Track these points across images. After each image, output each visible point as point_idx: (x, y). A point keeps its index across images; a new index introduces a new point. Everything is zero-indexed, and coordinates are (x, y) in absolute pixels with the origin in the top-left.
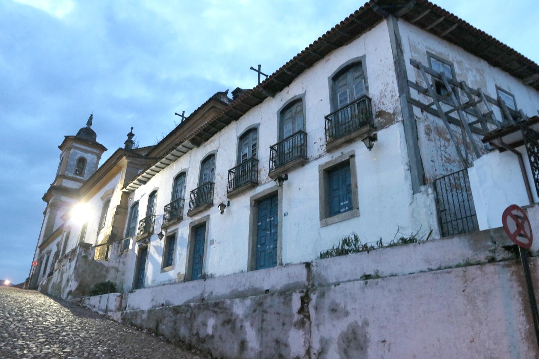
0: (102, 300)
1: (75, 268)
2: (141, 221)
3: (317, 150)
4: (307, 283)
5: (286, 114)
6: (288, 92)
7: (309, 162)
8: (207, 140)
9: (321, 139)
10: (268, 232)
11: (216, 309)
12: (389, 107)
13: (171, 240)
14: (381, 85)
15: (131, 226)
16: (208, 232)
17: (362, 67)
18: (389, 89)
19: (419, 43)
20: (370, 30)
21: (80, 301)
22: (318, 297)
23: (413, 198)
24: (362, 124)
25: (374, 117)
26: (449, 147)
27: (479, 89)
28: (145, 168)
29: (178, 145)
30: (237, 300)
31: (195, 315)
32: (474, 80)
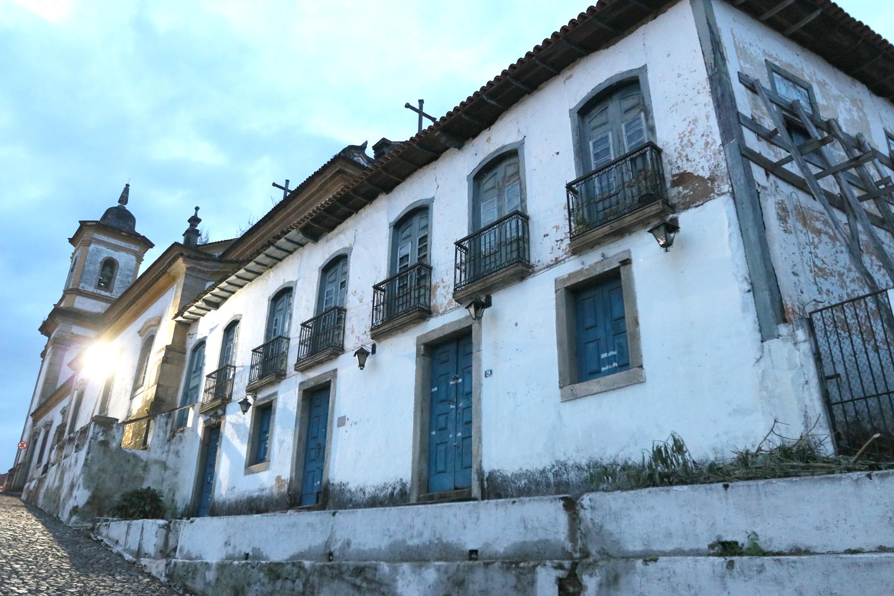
0: (131, 531)
1: (85, 465)
2: (209, 376)
3: (550, 250)
4: (569, 546)
5: (484, 181)
6: (488, 140)
7: (533, 272)
8: (332, 228)
9: (557, 227)
10: (452, 407)
11: (358, 581)
12: (700, 166)
13: (264, 414)
14: (683, 122)
15: (192, 385)
16: (334, 402)
17: (639, 88)
18: (700, 130)
19: (751, 46)
20: (655, 18)
21: (92, 529)
22: (600, 585)
23: (762, 349)
24: (646, 200)
25: (668, 185)
26: (821, 246)
27: (860, 135)
28: (219, 278)
29: (279, 238)
30: (406, 567)
31: (313, 587)
32: (848, 118)
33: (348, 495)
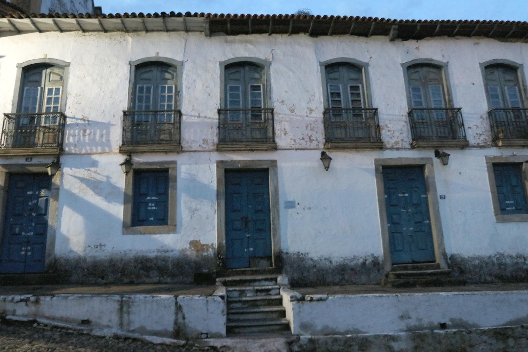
33: (310, 262)
